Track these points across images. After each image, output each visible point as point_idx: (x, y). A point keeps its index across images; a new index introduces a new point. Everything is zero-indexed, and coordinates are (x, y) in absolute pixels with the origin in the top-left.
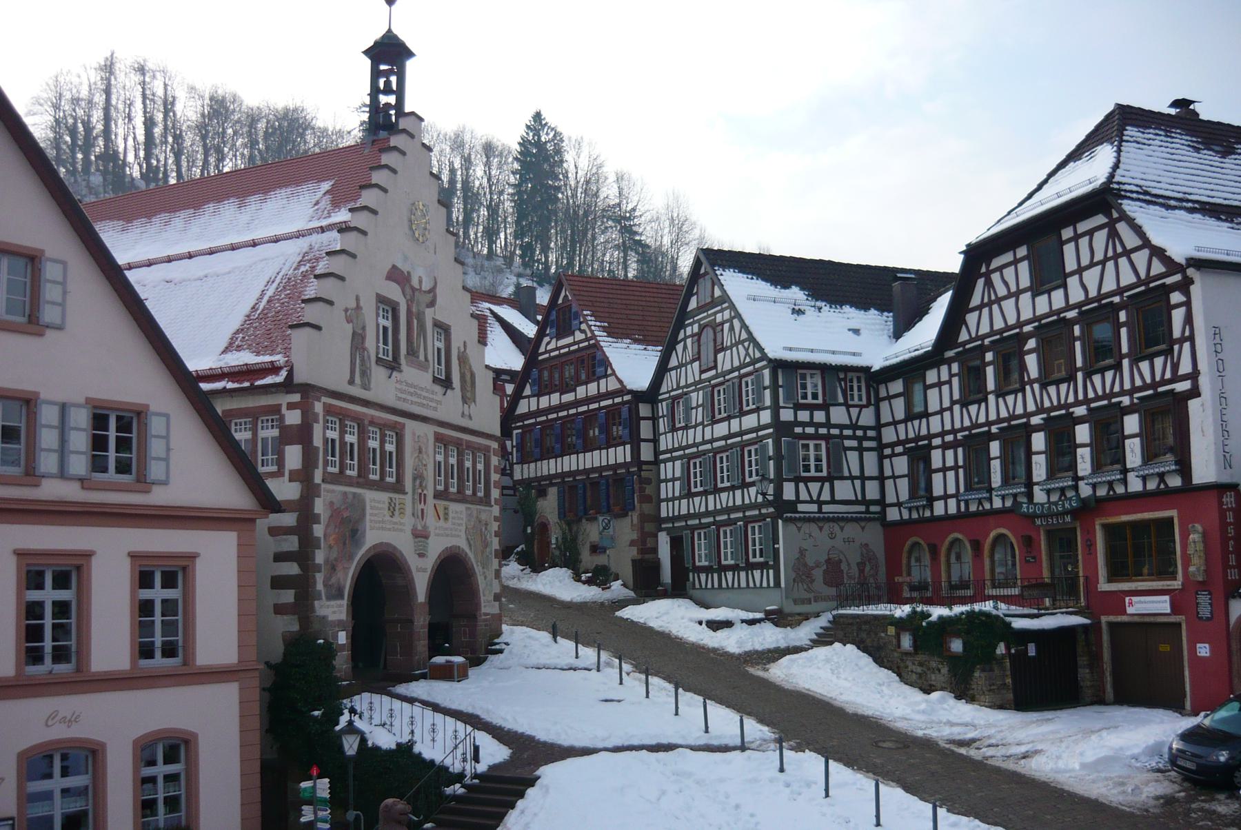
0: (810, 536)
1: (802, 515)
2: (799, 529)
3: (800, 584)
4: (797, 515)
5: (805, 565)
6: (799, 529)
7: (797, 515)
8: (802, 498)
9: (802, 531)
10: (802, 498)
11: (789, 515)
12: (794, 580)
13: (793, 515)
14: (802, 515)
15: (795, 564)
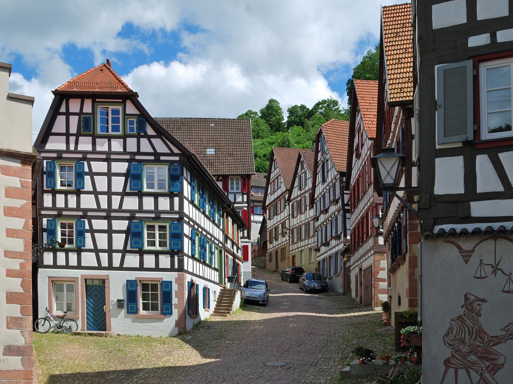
0: (495, 269)
1: (483, 226)
2: (466, 255)
3: (462, 373)
4: (470, 227)
5: (480, 332)
6: (466, 255)
7: (470, 227)
8: (480, 189)
9: (474, 260)
10: (480, 189)
11: (447, 227)
12: (447, 362)
13: (459, 227)
14: (483, 226)
15: (450, 330)
